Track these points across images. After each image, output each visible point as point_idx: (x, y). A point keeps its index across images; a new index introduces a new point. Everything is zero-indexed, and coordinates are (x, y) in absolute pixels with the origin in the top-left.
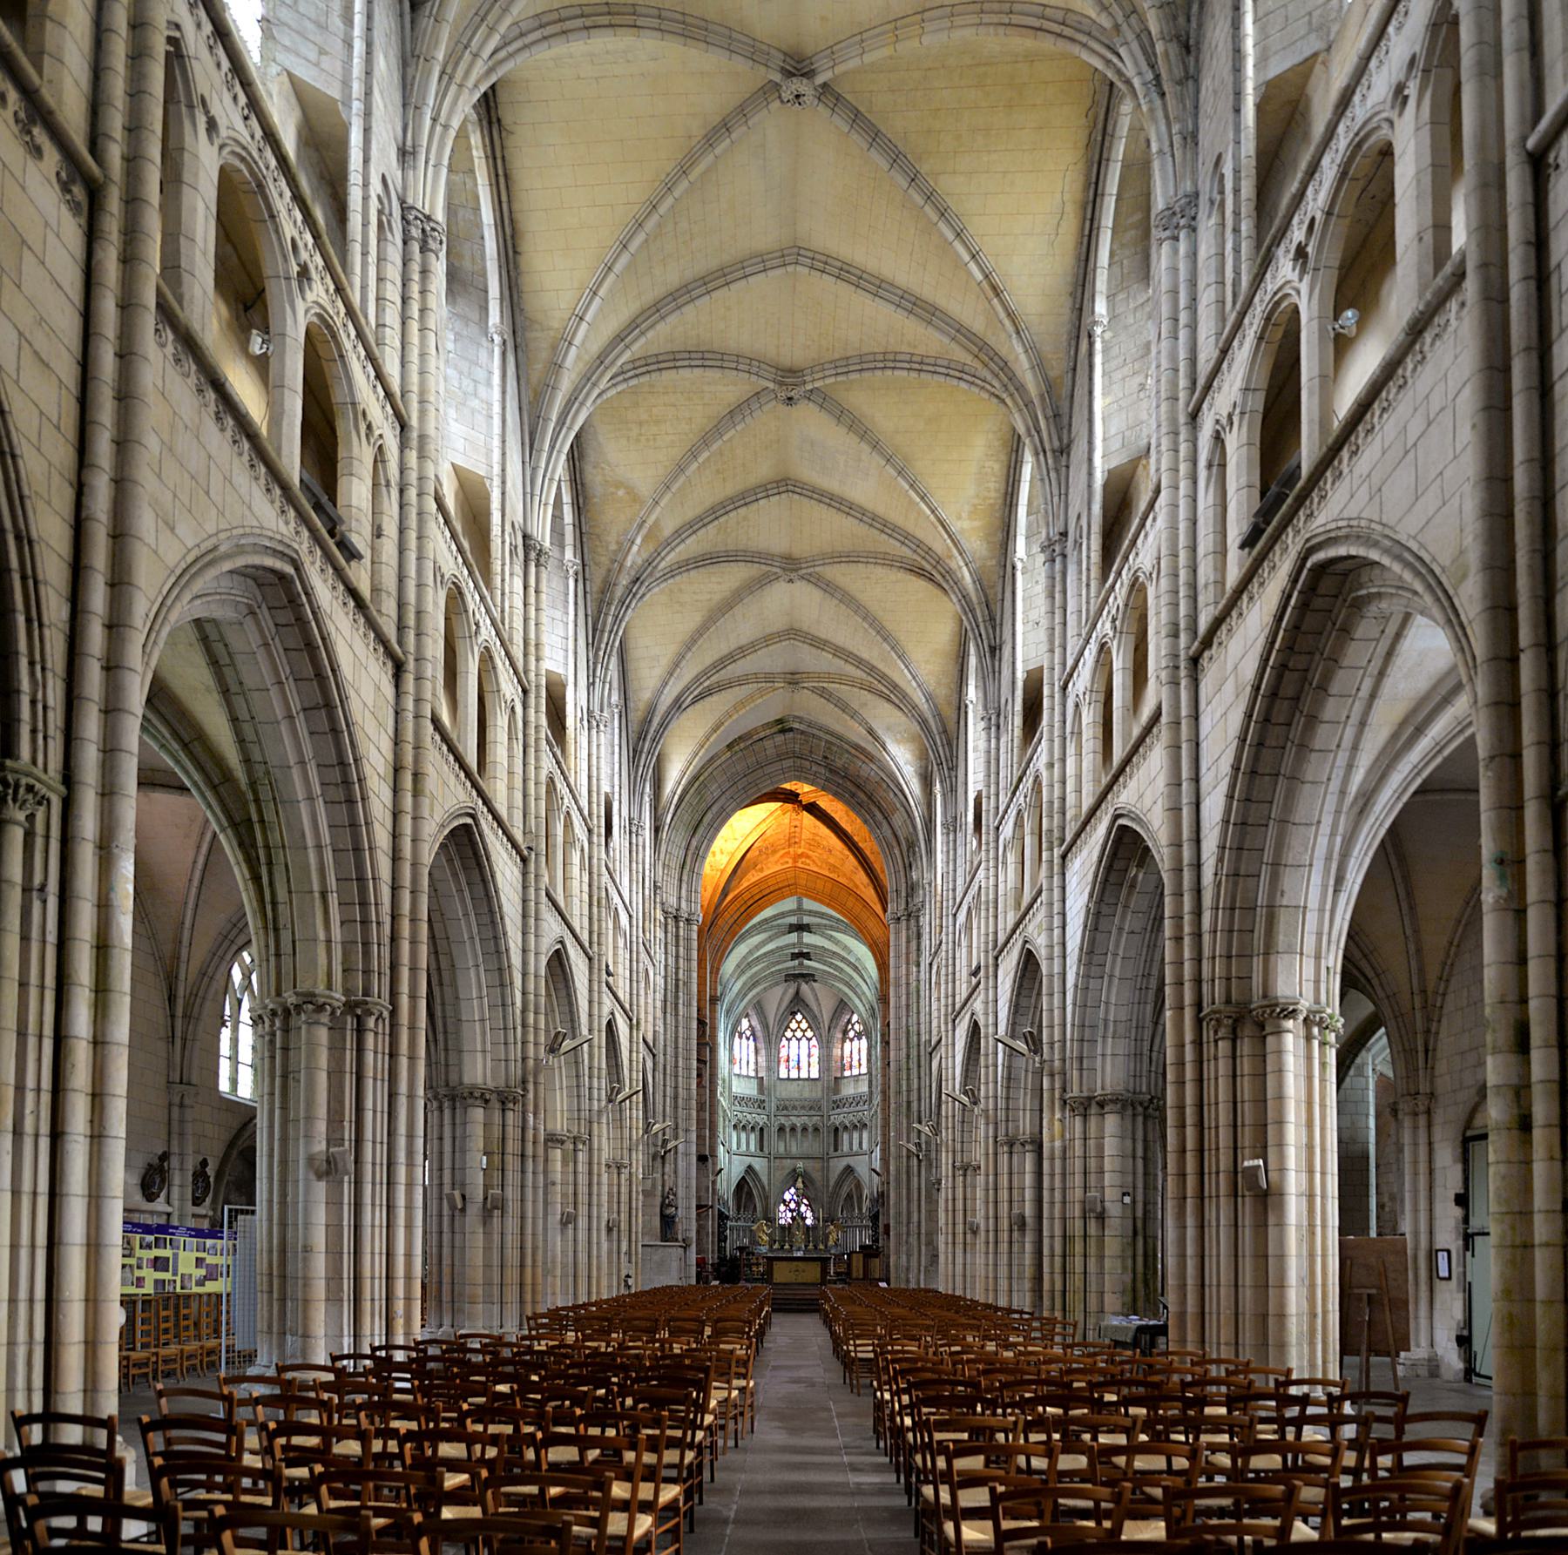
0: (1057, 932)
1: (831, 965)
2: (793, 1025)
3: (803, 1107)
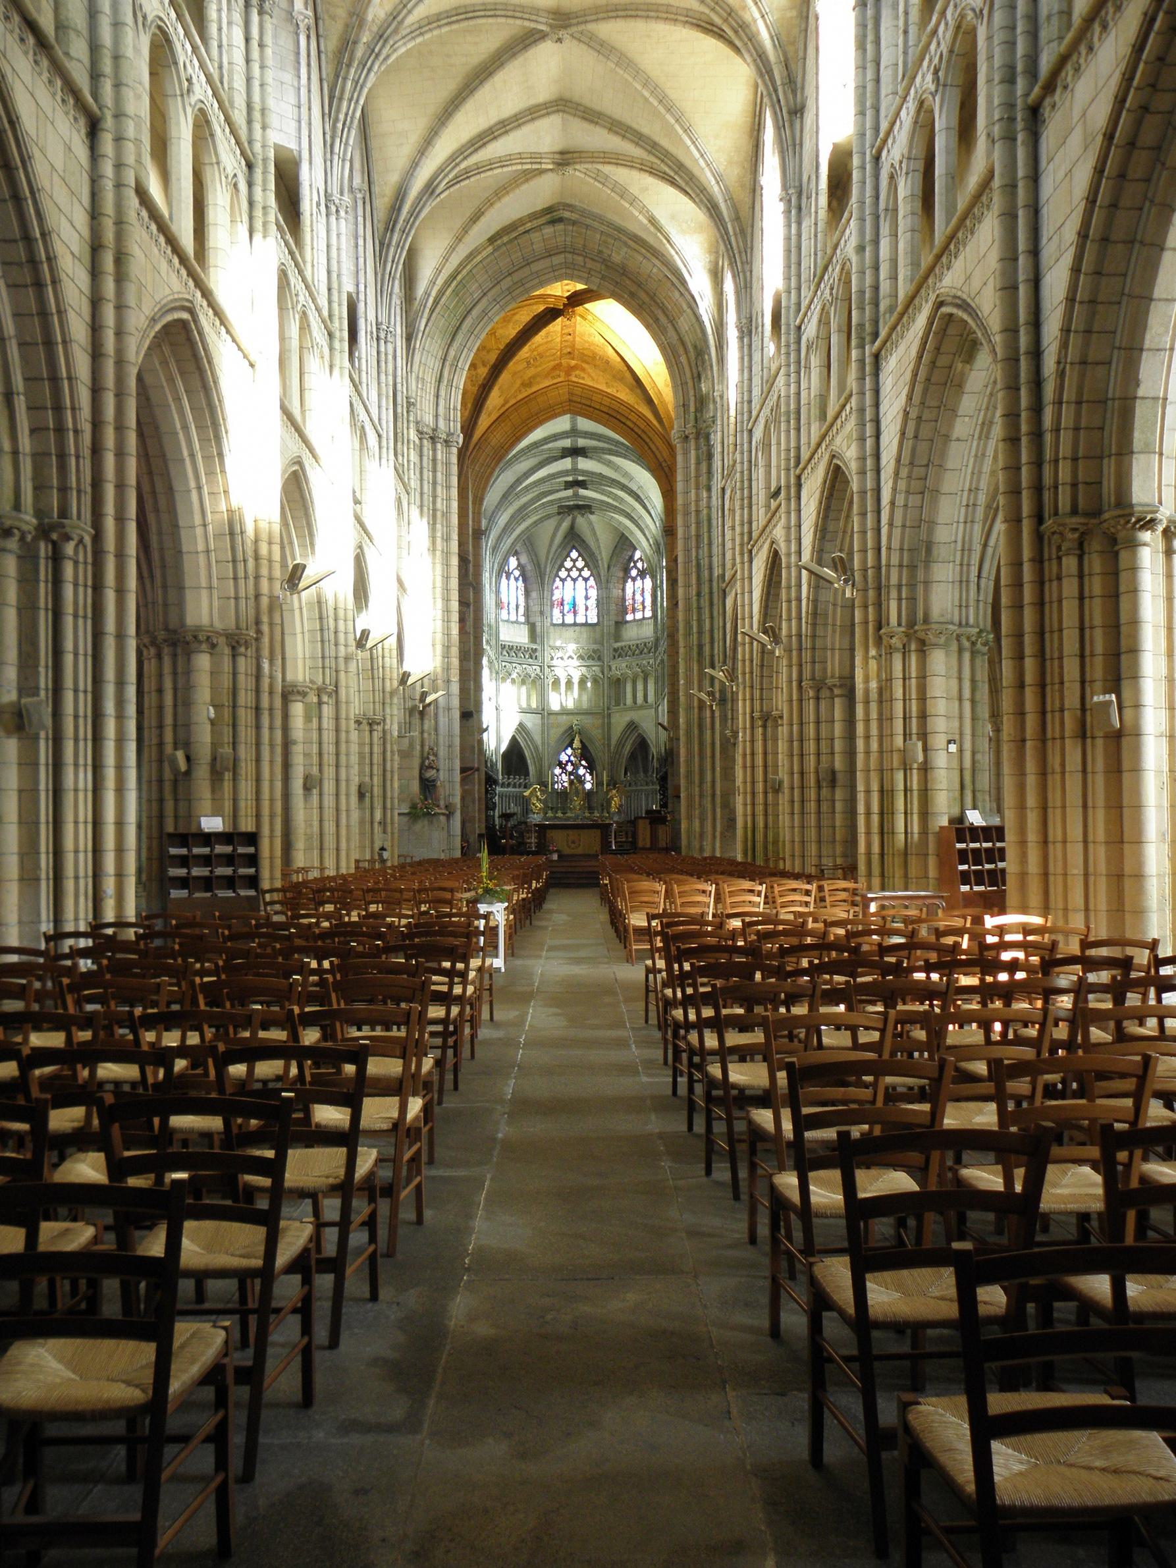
0: (869, 443)
1: (609, 495)
2: (568, 564)
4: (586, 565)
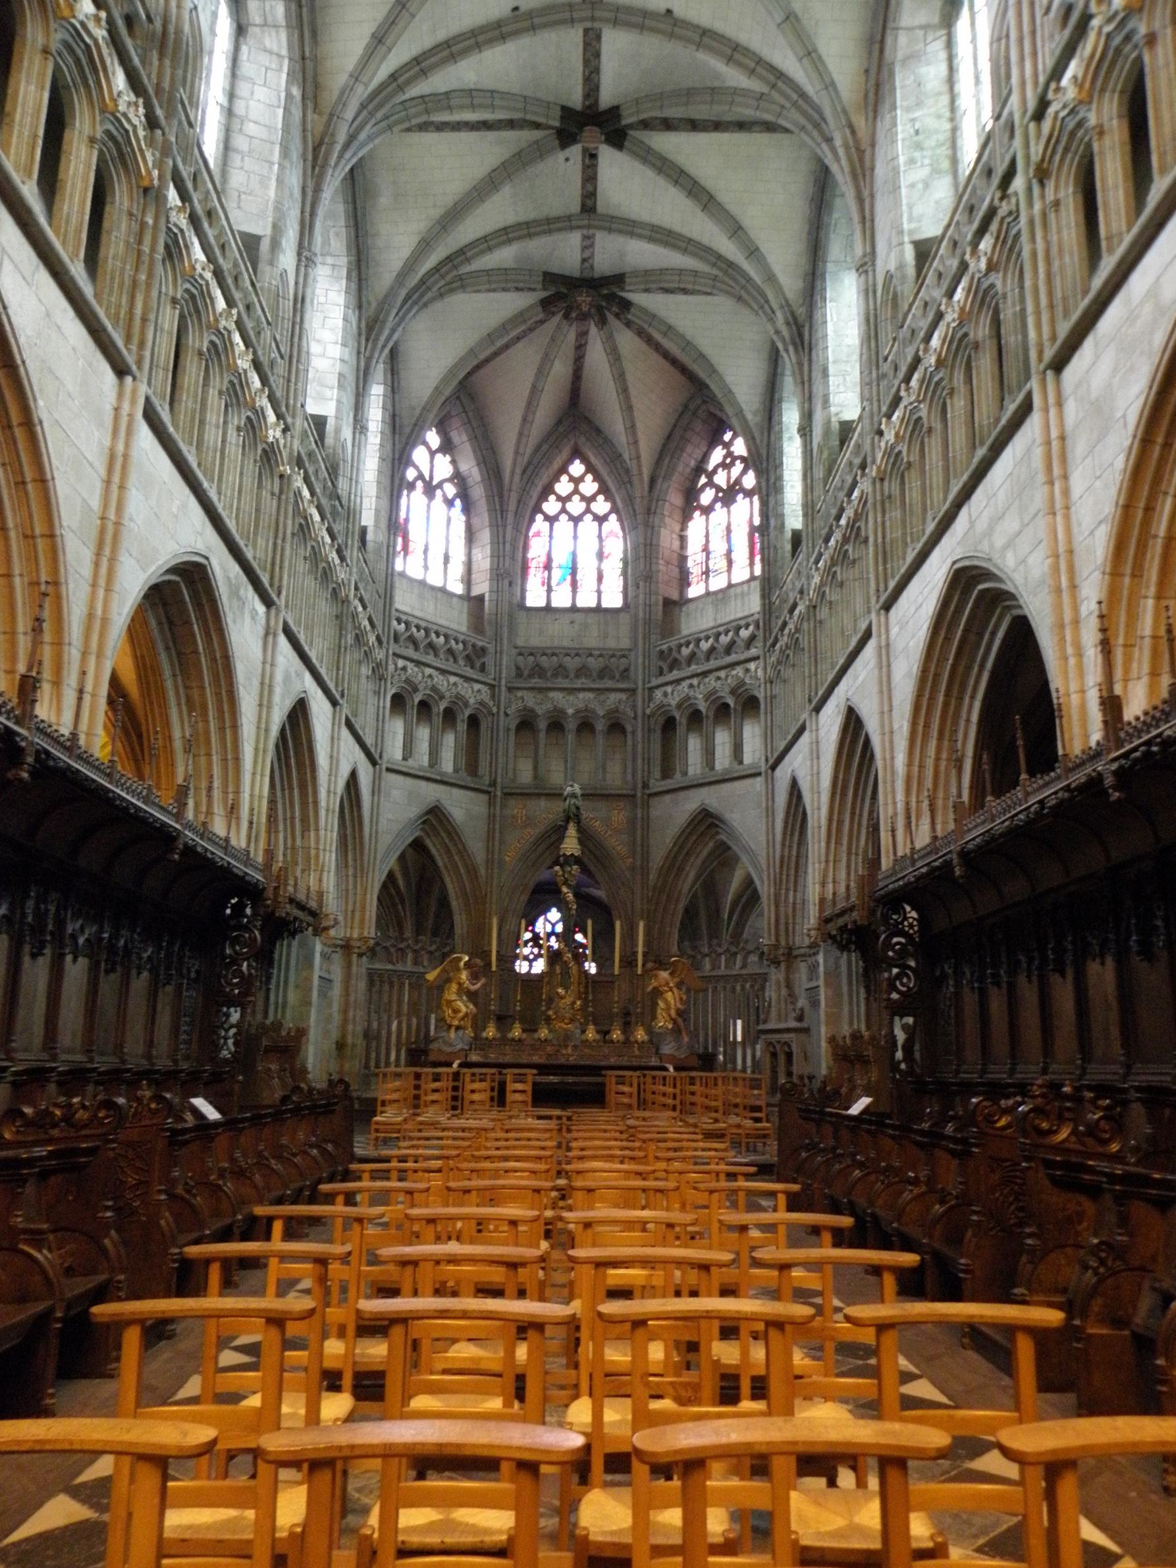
2: (563, 486)
3: (582, 671)
4: (604, 490)
